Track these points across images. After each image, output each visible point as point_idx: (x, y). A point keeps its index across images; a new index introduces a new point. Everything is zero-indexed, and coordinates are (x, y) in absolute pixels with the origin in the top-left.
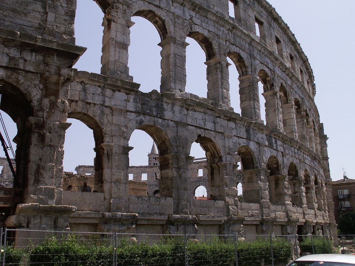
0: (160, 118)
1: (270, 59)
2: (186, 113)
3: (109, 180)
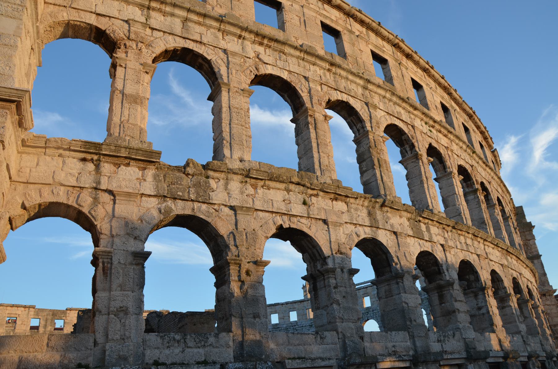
0: (204, 203)
1: (404, 108)
2: (252, 193)
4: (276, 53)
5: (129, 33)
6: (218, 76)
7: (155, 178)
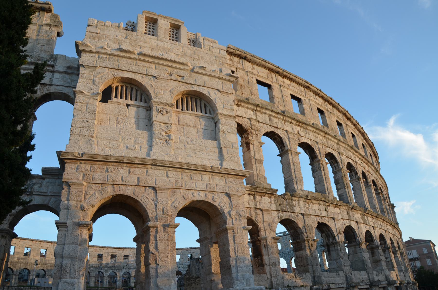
0: (292, 212)
3: (268, 264)
4: (304, 130)
5: (251, 125)
6: (285, 145)
7: (275, 202)
